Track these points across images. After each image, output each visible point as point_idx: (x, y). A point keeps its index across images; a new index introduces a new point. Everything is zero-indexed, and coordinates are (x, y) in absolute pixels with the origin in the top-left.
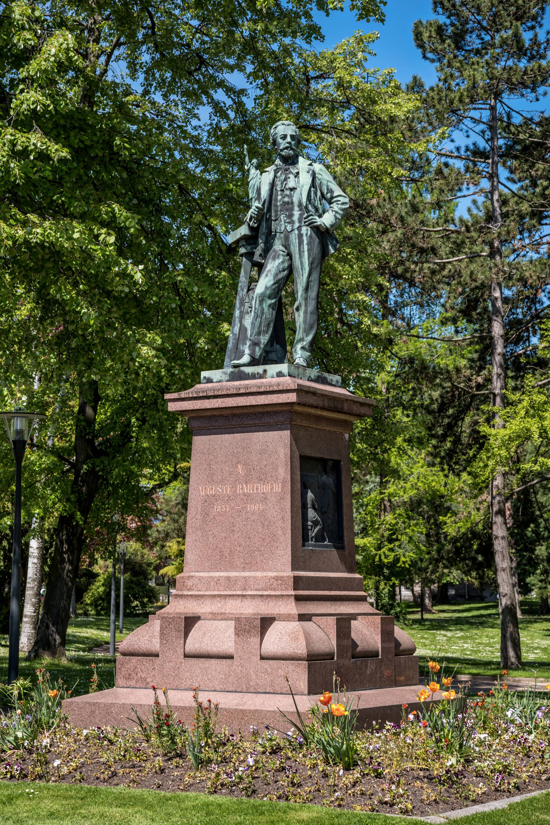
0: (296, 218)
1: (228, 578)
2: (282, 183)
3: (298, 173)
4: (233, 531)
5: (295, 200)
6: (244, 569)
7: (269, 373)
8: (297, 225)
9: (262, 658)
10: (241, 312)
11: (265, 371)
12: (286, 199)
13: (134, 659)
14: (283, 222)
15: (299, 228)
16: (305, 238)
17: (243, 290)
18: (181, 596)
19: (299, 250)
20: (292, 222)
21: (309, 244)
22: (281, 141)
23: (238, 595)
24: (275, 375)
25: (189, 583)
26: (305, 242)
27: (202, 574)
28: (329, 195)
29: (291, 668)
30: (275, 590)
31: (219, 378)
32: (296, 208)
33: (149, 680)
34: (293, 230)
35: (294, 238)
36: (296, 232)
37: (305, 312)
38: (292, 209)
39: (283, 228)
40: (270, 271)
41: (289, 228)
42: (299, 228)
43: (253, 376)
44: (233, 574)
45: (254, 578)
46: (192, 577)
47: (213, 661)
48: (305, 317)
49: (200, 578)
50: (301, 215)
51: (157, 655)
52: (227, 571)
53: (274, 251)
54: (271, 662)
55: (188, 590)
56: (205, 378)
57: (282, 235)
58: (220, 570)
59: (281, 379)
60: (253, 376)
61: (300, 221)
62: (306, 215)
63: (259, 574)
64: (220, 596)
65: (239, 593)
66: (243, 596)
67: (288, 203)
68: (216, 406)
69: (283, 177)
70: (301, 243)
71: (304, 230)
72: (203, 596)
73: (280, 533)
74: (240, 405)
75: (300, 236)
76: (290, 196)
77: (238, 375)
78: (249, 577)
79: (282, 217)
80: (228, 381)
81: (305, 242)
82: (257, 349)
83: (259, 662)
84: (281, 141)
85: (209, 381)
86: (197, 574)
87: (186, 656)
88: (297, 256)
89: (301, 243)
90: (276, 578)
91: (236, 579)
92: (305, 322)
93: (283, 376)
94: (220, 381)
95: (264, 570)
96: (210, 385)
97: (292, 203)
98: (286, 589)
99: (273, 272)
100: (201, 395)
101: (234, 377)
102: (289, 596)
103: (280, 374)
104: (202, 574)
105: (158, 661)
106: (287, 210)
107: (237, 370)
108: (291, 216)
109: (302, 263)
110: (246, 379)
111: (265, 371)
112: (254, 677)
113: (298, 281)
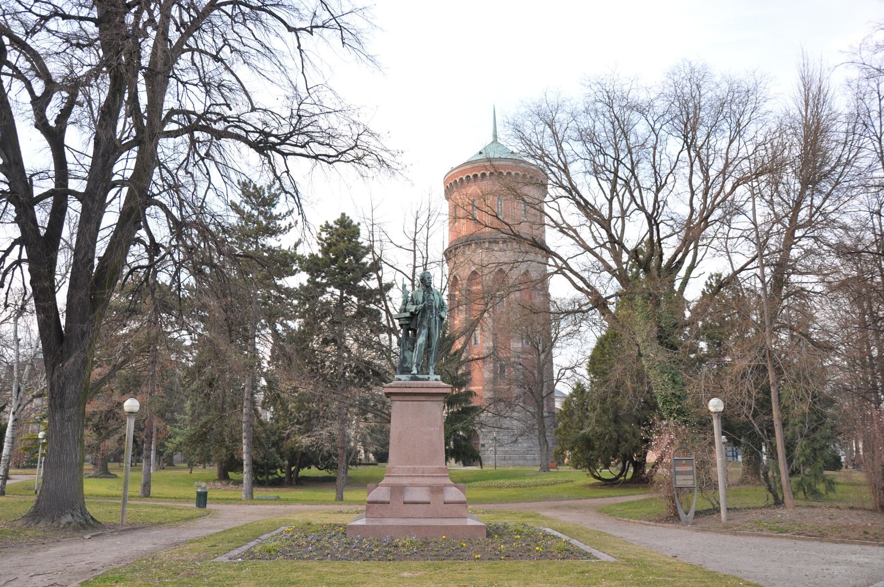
25: (393, 470)
43: (423, 380)
60: (423, 380)
85: (399, 380)
103: (436, 380)
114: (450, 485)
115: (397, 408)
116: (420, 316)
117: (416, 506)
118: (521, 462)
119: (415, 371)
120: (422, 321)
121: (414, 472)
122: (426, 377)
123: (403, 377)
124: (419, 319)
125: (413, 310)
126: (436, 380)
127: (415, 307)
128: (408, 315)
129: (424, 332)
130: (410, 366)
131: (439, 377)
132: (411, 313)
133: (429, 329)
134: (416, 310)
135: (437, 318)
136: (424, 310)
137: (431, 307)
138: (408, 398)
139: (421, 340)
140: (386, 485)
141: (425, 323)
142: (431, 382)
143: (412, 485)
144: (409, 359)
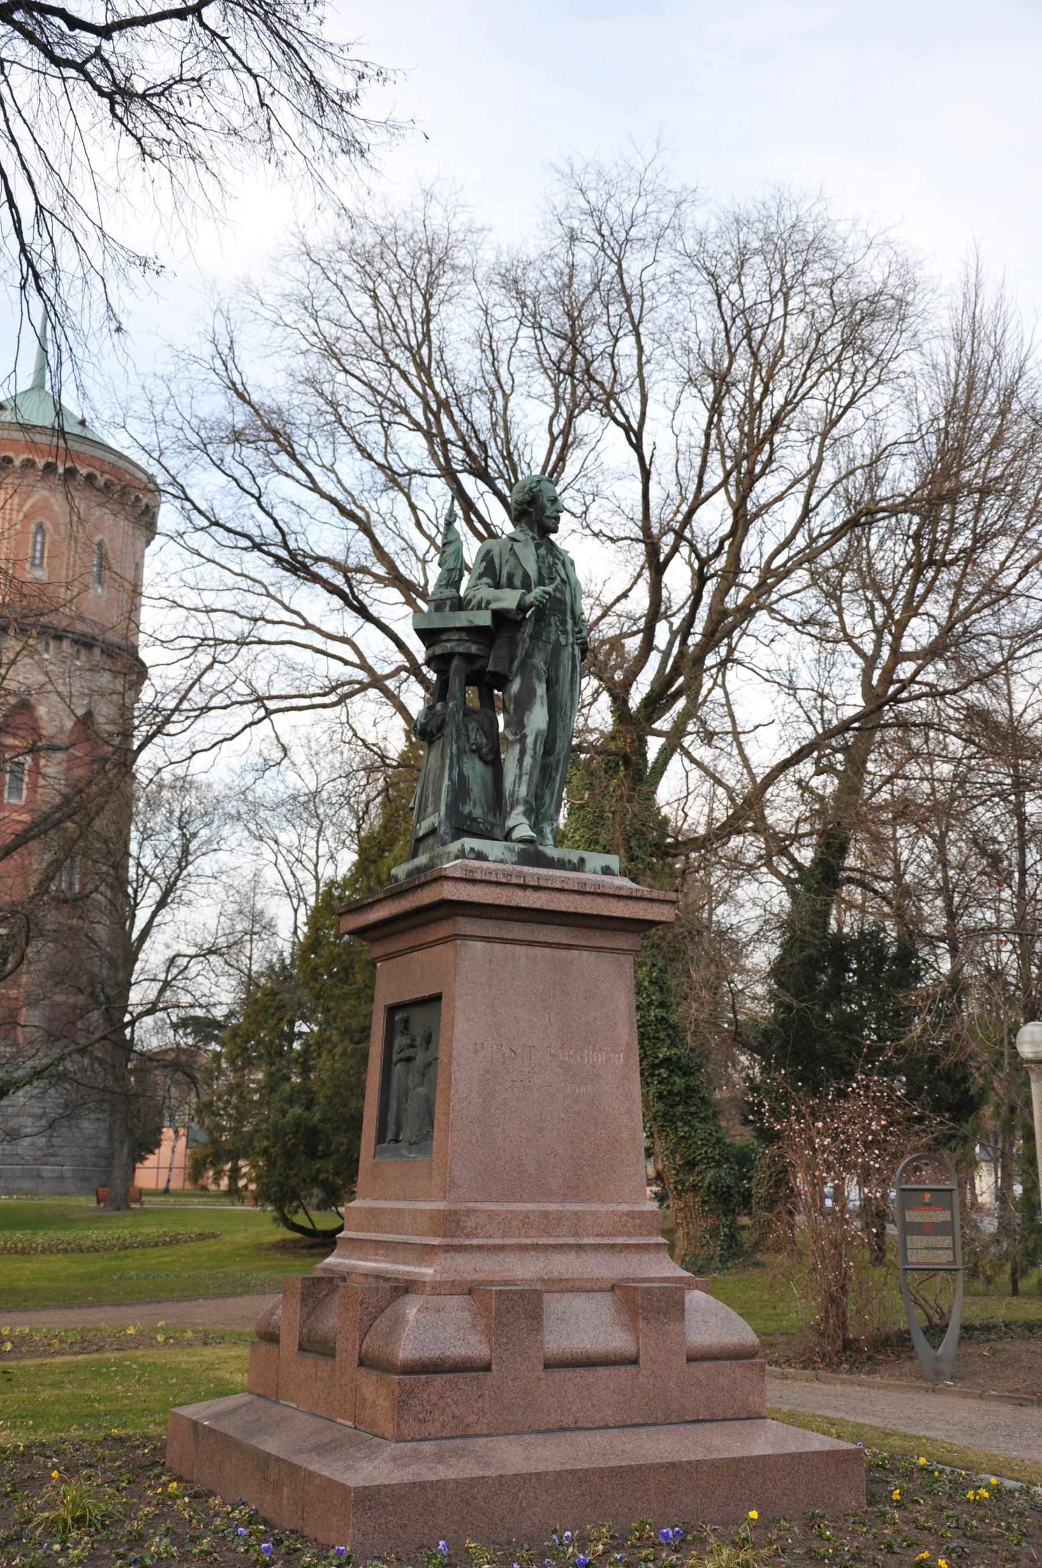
1: (546, 1214)
6: (565, 1198)
9: (690, 1360)
11: (582, 860)
13: (438, 1380)
20: (565, 632)
22: (548, 504)
23: (571, 1246)
25: (470, 1223)
27: (492, 1207)
30: (629, 1235)
38: (565, 614)
39: (553, 638)
43: (561, 864)
44: (553, 1207)
45: (594, 1214)
46: (475, 1211)
47: (601, 1371)
49: (491, 1214)
51: (487, 1368)
52: (533, 1201)
54: (706, 1365)
55: (468, 1236)
56: (472, 850)
57: (549, 647)
59: (608, 879)
60: (561, 864)
63: (595, 1207)
64: (536, 1247)
65: (571, 1241)
66: (580, 1247)
68: (538, 905)
71: (576, 647)
74: (580, 911)
75: (574, 656)
77: (531, 855)
78: (584, 1213)
80: (516, 863)
83: (685, 1366)
84: (548, 504)
85: (481, 856)
86: (479, 1206)
87: (549, 1365)
88: (567, 686)
90: (632, 1215)
93: (612, 874)
94: (501, 861)
95: (602, 1201)
96: (477, 864)
98: (650, 1234)
100: (514, 881)
102: (658, 1246)
103: (607, 871)
104: (492, 1207)
105: (489, 1379)
108: (564, 623)
110: (548, 867)
111: (582, 860)
116: (528, 629)
118: (26, 1184)
120: (529, 655)
121: (546, 1232)
126: (607, 871)
128: (484, 619)
131: (613, 861)
134: (522, 608)
136: (542, 612)
138: (516, 930)
141: (539, 661)
142: (589, 877)
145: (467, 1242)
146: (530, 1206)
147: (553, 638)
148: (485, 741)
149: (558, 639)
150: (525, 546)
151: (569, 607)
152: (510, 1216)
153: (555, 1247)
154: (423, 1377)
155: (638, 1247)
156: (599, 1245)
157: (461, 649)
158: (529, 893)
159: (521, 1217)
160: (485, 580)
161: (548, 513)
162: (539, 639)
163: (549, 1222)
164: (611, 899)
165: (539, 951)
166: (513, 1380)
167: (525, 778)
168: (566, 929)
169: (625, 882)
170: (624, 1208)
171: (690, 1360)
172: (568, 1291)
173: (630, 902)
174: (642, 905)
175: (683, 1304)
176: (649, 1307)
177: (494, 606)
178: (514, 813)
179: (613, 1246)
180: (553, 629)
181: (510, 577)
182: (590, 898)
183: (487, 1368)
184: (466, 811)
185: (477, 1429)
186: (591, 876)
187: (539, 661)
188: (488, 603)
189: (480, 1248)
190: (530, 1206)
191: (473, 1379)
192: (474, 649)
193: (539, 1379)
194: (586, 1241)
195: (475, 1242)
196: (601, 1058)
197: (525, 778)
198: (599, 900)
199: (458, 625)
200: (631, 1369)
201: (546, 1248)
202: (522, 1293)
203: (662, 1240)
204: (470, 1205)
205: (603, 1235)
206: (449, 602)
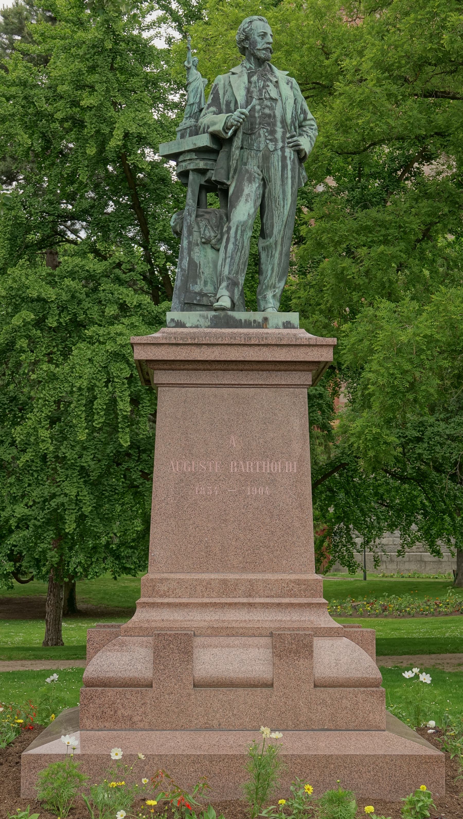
0: (279, 135)
1: (225, 582)
2: (260, 91)
3: (277, 82)
4: (225, 520)
5: (278, 113)
6: (244, 570)
7: (271, 322)
8: (280, 145)
9: (315, 686)
10: (190, 243)
11: (266, 319)
12: (267, 111)
13: (110, 692)
14: (262, 139)
15: (283, 149)
16: (289, 162)
17: (190, 215)
18: (153, 605)
19: (282, 175)
20: (274, 140)
21: (293, 170)
22: (259, 39)
23: (243, 604)
24: (280, 324)
26: (289, 167)
27: (182, 576)
28: (302, 115)
29: (360, 697)
30: (295, 596)
31: (196, 323)
32: (279, 124)
33: (136, 719)
34: (276, 149)
35: (276, 159)
36: (280, 153)
37: (281, 254)
38: (274, 125)
39: (262, 146)
40: (248, 195)
41: (271, 146)
42: (283, 149)
43: (248, 324)
45: (264, 581)
46: (167, 579)
47: (240, 691)
48: (280, 259)
49: (179, 582)
50: (284, 133)
51: (150, 686)
52: (218, 572)
53: (247, 171)
54: (330, 690)
55: (161, 596)
56: (173, 320)
57: (260, 154)
58: (207, 571)
60: (248, 324)
61: (283, 141)
62: (288, 135)
65: (245, 600)
67: (269, 116)
68: (212, 358)
69: (261, 84)
70: (284, 167)
72: (186, 605)
73: (297, 524)
74: (248, 359)
75: (284, 158)
76: (272, 108)
79: (261, 132)
80: (208, 327)
81: (289, 167)
82: (236, 291)
84: (259, 39)
85: (180, 324)
86: (172, 576)
88: (279, 182)
89: (284, 167)
90: (298, 582)
91: (237, 583)
92: (279, 264)
93: (294, 327)
94: (197, 327)
97: (275, 116)
98: (313, 596)
99: (253, 196)
101: (216, 323)
102: (320, 605)
103: (288, 325)
104: (182, 576)
105: (150, 693)
106: (269, 124)
107: (222, 313)
108: (273, 132)
109: (284, 192)
111: (266, 319)
112: (305, 710)
113: (276, 213)
114: (329, 633)
115: (173, 403)
116: (237, 142)
117: (231, 694)
119: (225, 302)
122: (258, 316)
123: (192, 317)
124: (236, 152)
125: (219, 127)
126: (288, 325)
127: (222, 117)
128: (204, 140)
129: (251, 190)
130: (209, 288)
131: (294, 317)
132: (215, 136)
133: (265, 182)
134: (226, 128)
135: (289, 152)
136: (248, 127)
137: (269, 121)
138: (205, 377)
139: (244, 211)
140: (142, 631)
141: (253, 166)
143: (216, 631)
144: (206, 271)
145: (159, 600)
146: (213, 576)
147: (262, 146)
148: (213, 234)
149: (267, 146)
150: (240, 76)
151: (279, 118)
152: (195, 583)
153: (230, 604)
154: (100, 689)
155: (300, 605)
156: (267, 604)
157: (192, 167)
158: (204, 349)
159: (204, 584)
160: (213, 109)
161: (259, 47)
162: (250, 148)
163: (226, 587)
164: (275, 348)
165: (225, 391)
166: (168, 694)
167: (228, 260)
168: (246, 373)
169: (303, 334)
170: (294, 577)
171: (315, 686)
172: (233, 636)
173: (292, 349)
174: (303, 350)
175: (312, 647)
176: (293, 647)
177: (211, 130)
178: (221, 287)
179: (279, 605)
180: (262, 139)
181: (228, 104)
182: (257, 348)
183: (150, 686)
184: (197, 288)
185: (141, 725)
186: (277, 331)
187: (253, 166)
188: (208, 127)
189: (169, 605)
190: (213, 576)
191: (137, 692)
192: (201, 165)
193: (190, 695)
194: (258, 600)
195: (166, 600)
196: (278, 467)
197: (228, 260)
198: (265, 349)
199: (187, 148)
200: (266, 691)
201: (223, 605)
202: (176, 636)
203: (324, 601)
204: (166, 575)
205: (273, 597)
206: (188, 130)
